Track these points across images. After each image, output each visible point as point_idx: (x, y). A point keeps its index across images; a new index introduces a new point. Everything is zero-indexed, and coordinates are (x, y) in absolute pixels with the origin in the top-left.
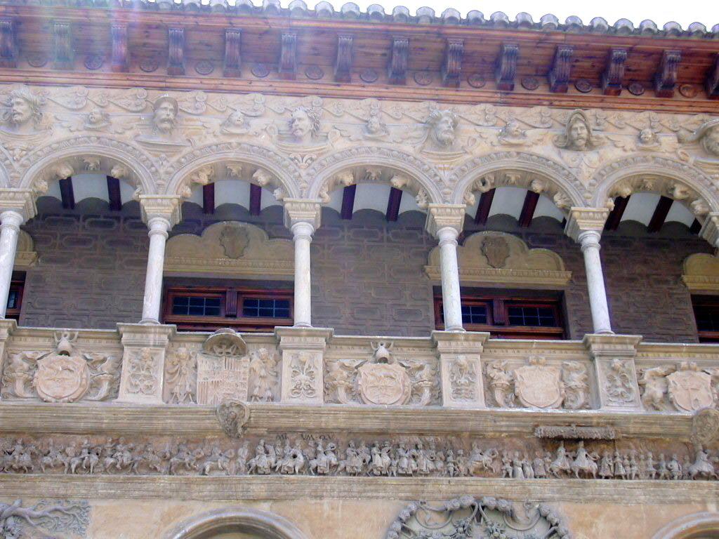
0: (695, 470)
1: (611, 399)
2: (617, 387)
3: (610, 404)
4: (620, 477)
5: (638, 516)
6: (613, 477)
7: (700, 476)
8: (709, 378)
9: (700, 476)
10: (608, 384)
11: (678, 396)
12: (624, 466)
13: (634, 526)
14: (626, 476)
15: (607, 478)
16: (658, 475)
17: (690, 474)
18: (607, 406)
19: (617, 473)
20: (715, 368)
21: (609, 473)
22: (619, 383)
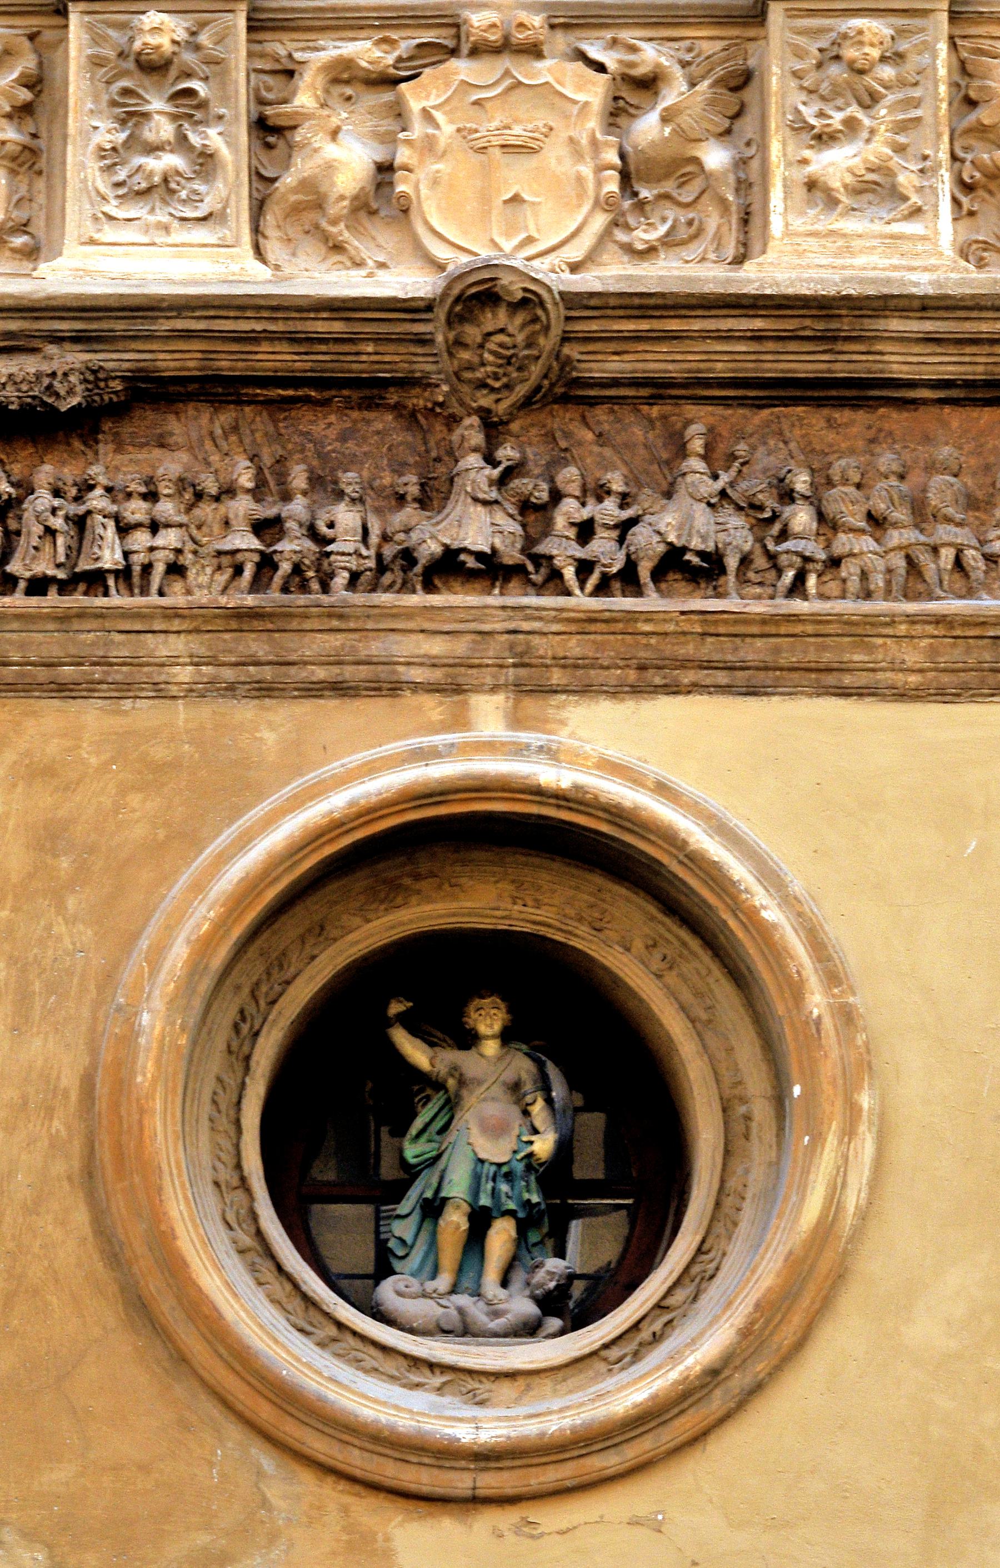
0: (430, 539)
1: (111, 209)
2: (153, 149)
3: (109, 233)
4: (95, 581)
5: (160, 753)
6: (65, 587)
7: (448, 567)
8: (593, 93)
9: (448, 567)
10: (108, 133)
11: (435, 182)
12: (124, 529)
13: (135, 799)
14: (124, 574)
15: (38, 586)
16: (267, 563)
17: (408, 557)
18: (92, 242)
19: (84, 565)
20: (626, 35)
21: (44, 567)
22: (163, 129)
